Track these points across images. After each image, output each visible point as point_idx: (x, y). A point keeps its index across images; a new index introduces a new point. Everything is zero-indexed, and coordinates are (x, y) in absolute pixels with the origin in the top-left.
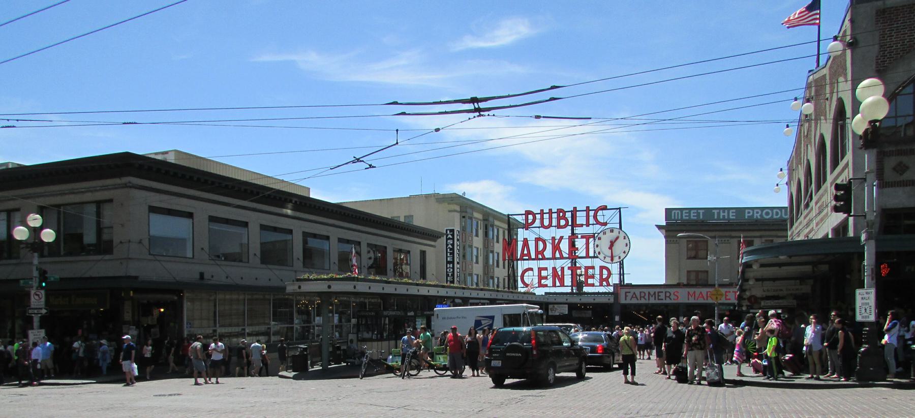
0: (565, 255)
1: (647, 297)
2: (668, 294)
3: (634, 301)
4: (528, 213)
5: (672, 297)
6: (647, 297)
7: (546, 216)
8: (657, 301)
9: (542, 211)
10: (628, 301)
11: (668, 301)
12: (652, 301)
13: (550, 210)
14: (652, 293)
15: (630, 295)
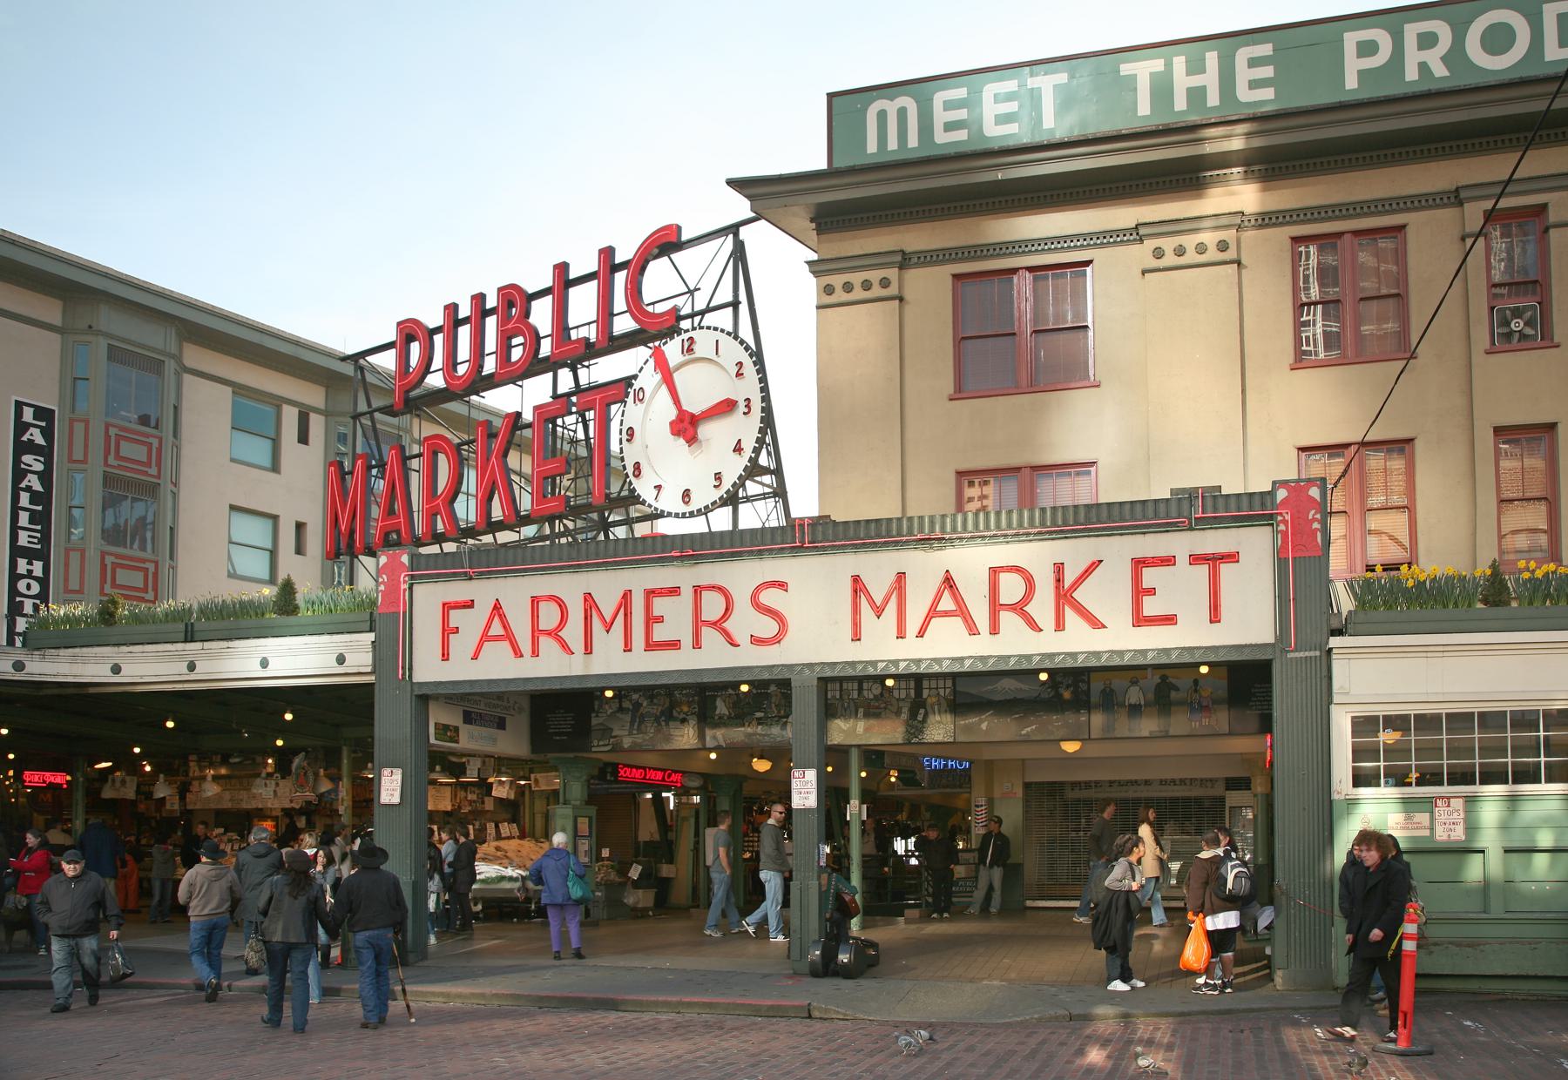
0: (526, 503)
1: (573, 632)
2: (713, 606)
3: (498, 666)
4: (410, 331)
5: (746, 622)
6: (573, 632)
7: (464, 333)
8: (643, 663)
9: (452, 309)
10: (462, 669)
11: (713, 657)
12: (612, 659)
13: (479, 299)
14: (608, 605)
15: (470, 624)
